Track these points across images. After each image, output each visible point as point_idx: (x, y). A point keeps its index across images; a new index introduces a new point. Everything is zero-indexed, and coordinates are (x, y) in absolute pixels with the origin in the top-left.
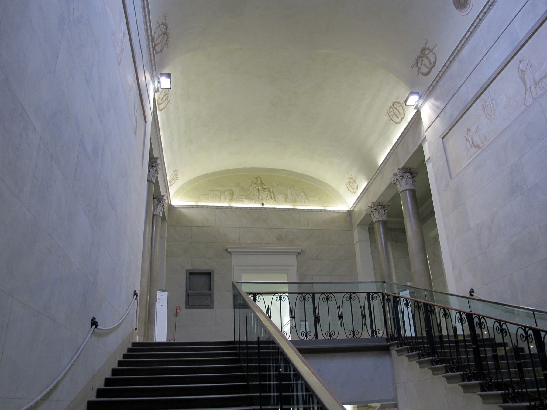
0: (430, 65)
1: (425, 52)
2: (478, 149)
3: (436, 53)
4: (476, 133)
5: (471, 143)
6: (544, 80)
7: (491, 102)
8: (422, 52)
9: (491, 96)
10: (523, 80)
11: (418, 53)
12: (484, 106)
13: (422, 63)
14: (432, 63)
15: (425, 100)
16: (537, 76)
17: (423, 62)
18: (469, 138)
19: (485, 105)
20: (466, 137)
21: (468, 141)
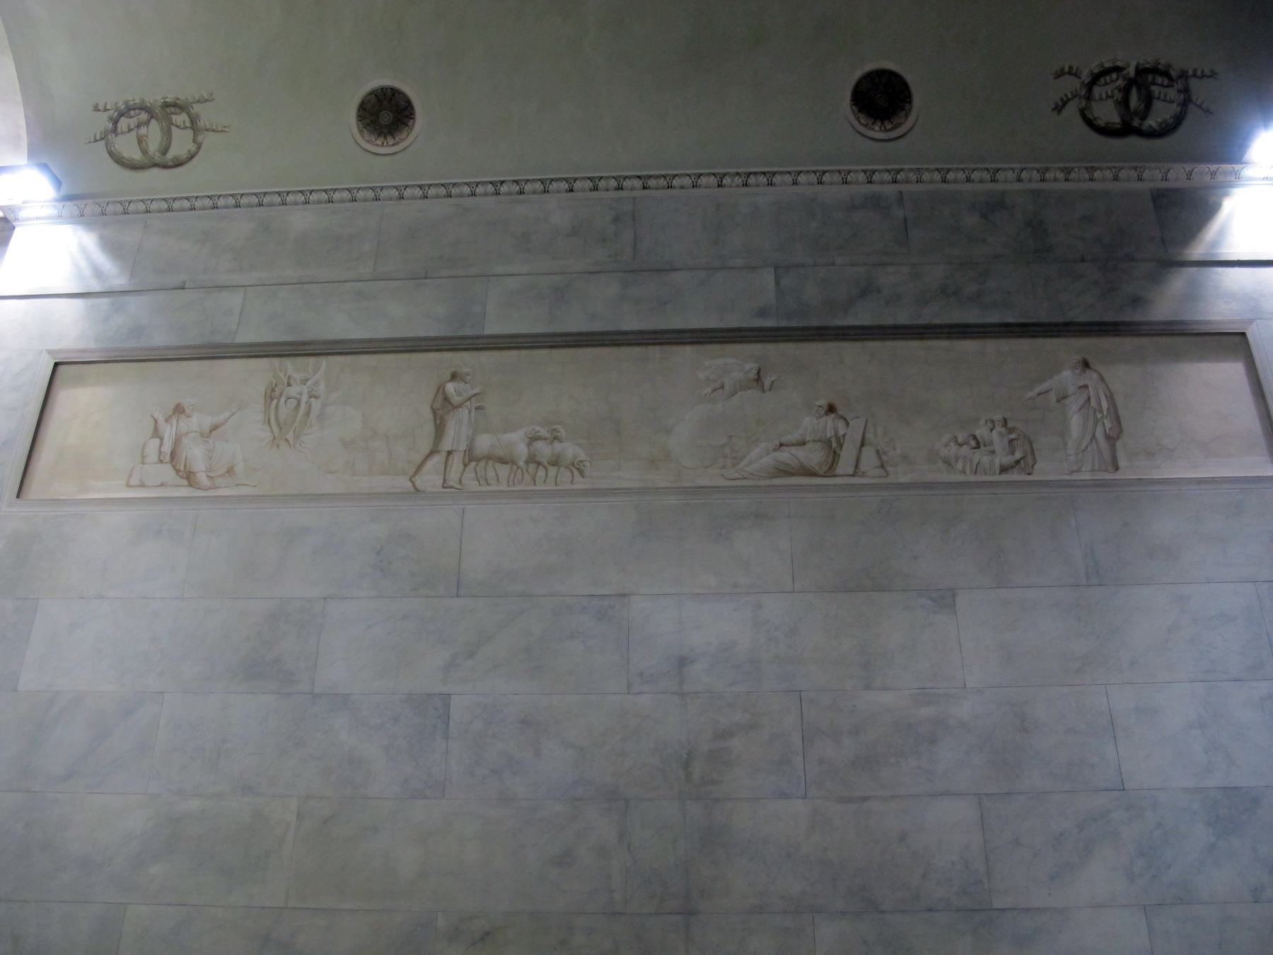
0: (158, 154)
1: (176, 114)
2: (185, 482)
3: (204, 147)
4: (202, 435)
5: (167, 448)
6: (498, 465)
7: (305, 398)
8: (166, 105)
9: (316, 384)
10: (438, 422)
11: (155, 97)
12: (273, 390)
13: (138, 126)
14: (171, 154)
15: (60, 216)
16: (484, 443)
17: (143, 130)
18: (169, 432)
19: (281, 395)
20: (156, 421)
21: (156, 433)
